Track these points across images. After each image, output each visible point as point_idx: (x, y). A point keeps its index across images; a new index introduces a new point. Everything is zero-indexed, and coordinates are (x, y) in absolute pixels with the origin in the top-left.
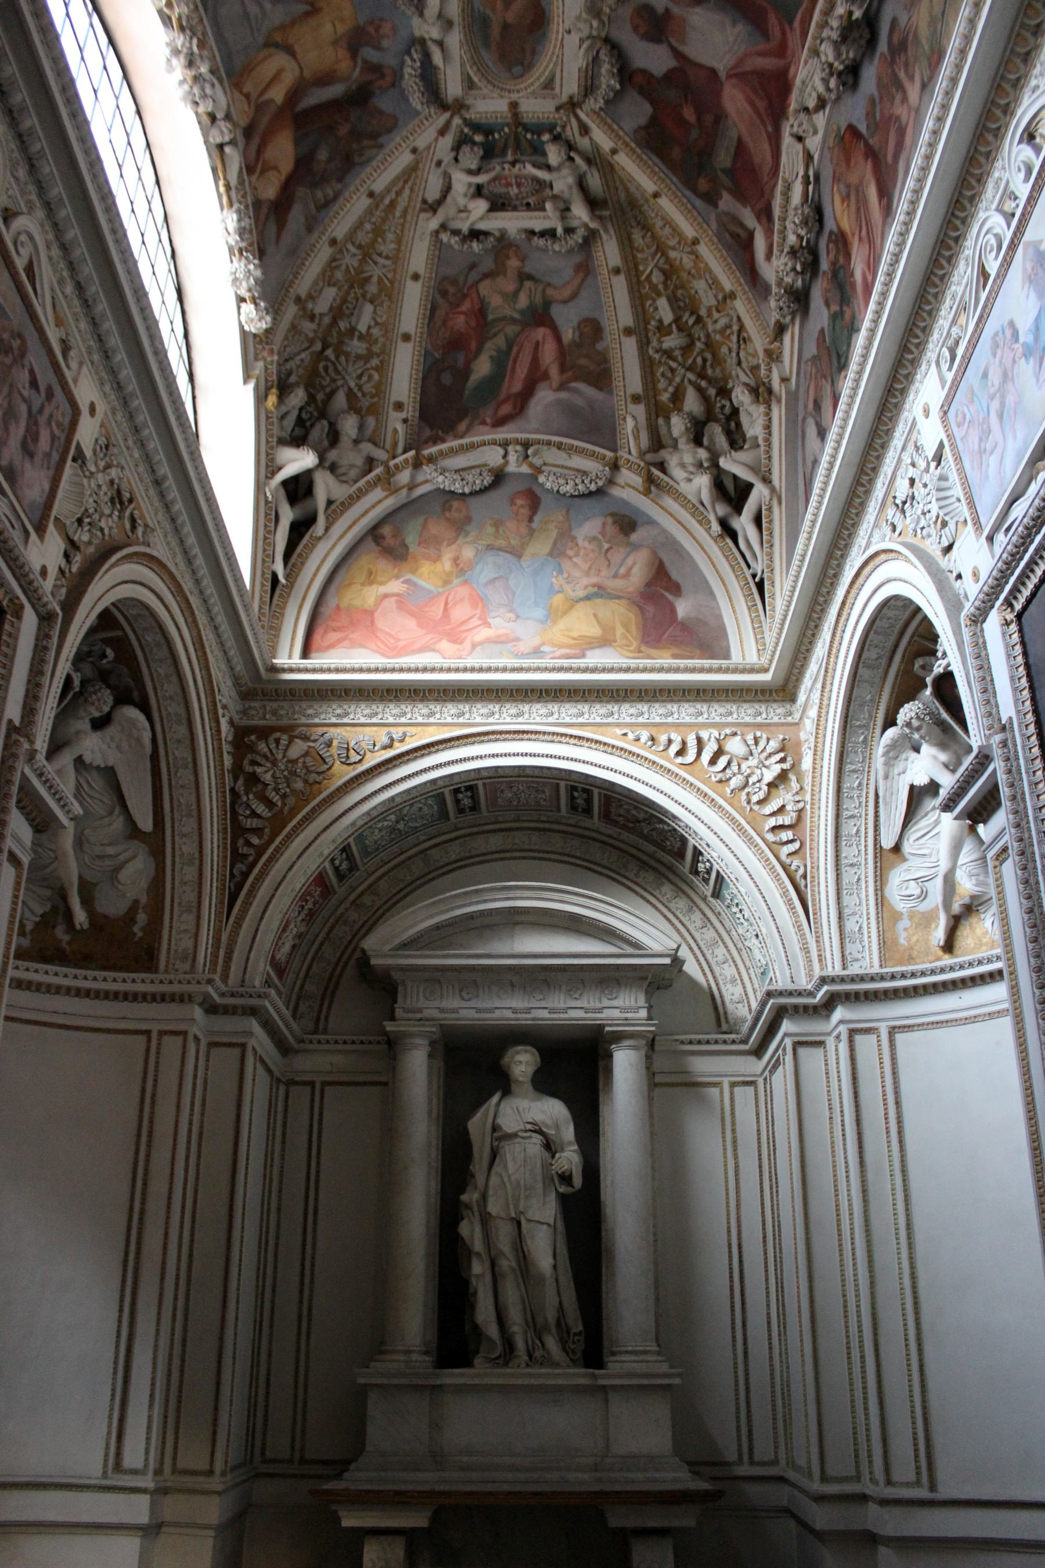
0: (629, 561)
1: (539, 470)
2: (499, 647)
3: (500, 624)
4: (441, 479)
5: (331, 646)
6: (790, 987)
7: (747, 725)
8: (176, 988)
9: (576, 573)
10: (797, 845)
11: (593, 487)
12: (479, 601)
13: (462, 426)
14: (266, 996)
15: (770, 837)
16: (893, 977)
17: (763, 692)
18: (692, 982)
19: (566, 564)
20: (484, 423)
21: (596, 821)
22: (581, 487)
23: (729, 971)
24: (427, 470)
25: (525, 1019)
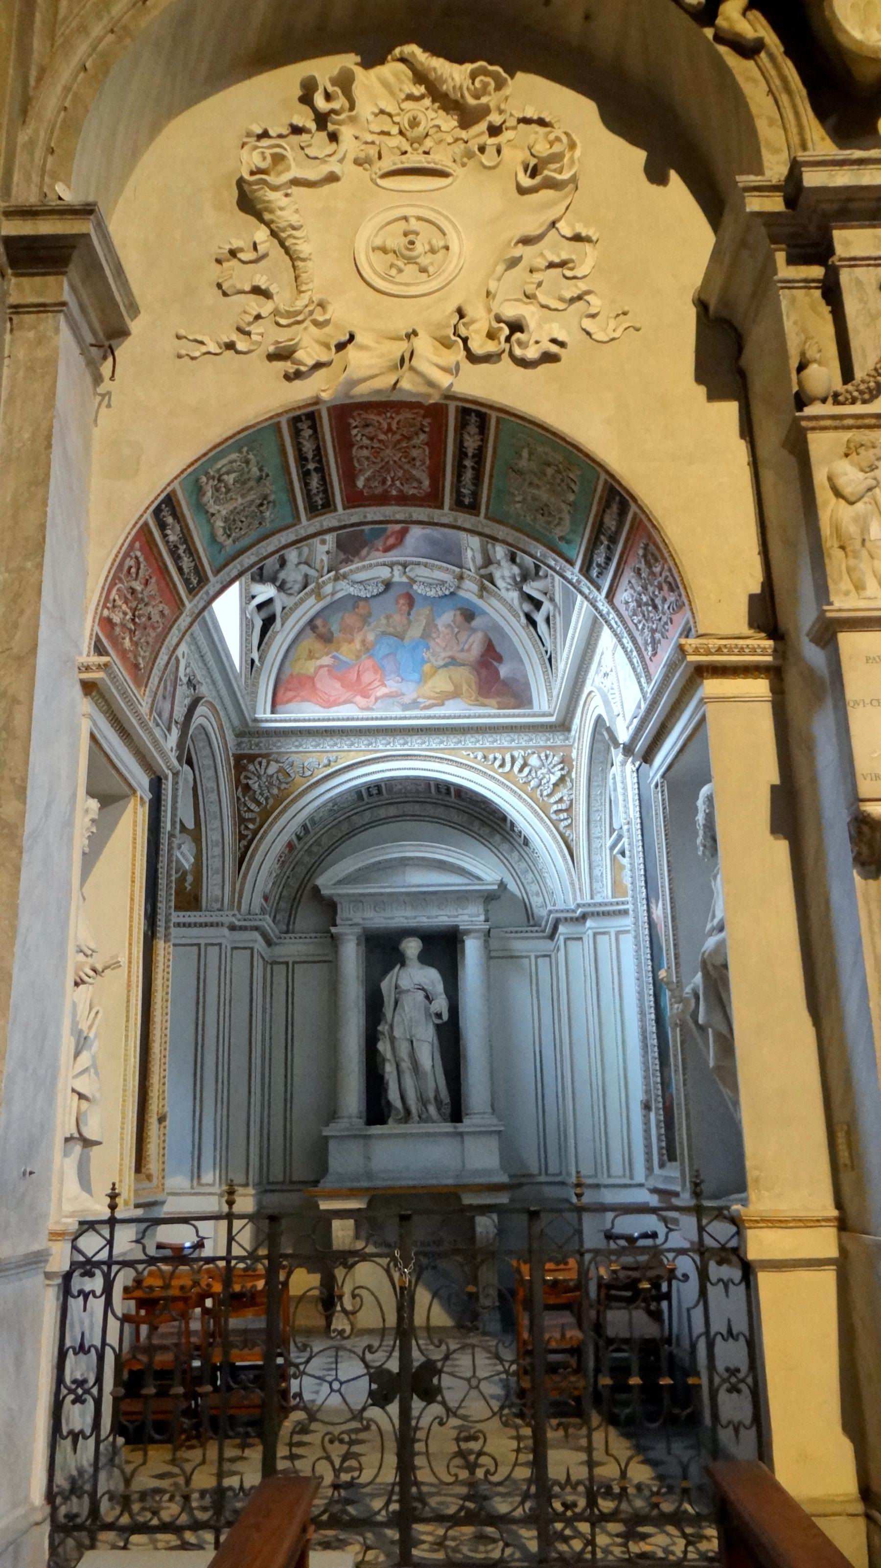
0: (471, 640)
1: (413, 581)
2: (391, 700)
3: (392, 685)
4: (352, 589)
5: (289, 701)
6: (563, 907)
7: (541, 747)
8: (214, 919)
9: (438, 649)
10: (569, 821)
11: (447, 593)
12: (379, 669)
13: (364, 552)
14: (264, 920)
15: (554, 817)
16: (617, 904)
17: (551, 727)
18: (513, 895)
19: (432, 644)
20: (378, 550)
21: (453, 798)
22: (440, 593)
23: (534, 888)
24: (342, 584)
25: (412, 923)
